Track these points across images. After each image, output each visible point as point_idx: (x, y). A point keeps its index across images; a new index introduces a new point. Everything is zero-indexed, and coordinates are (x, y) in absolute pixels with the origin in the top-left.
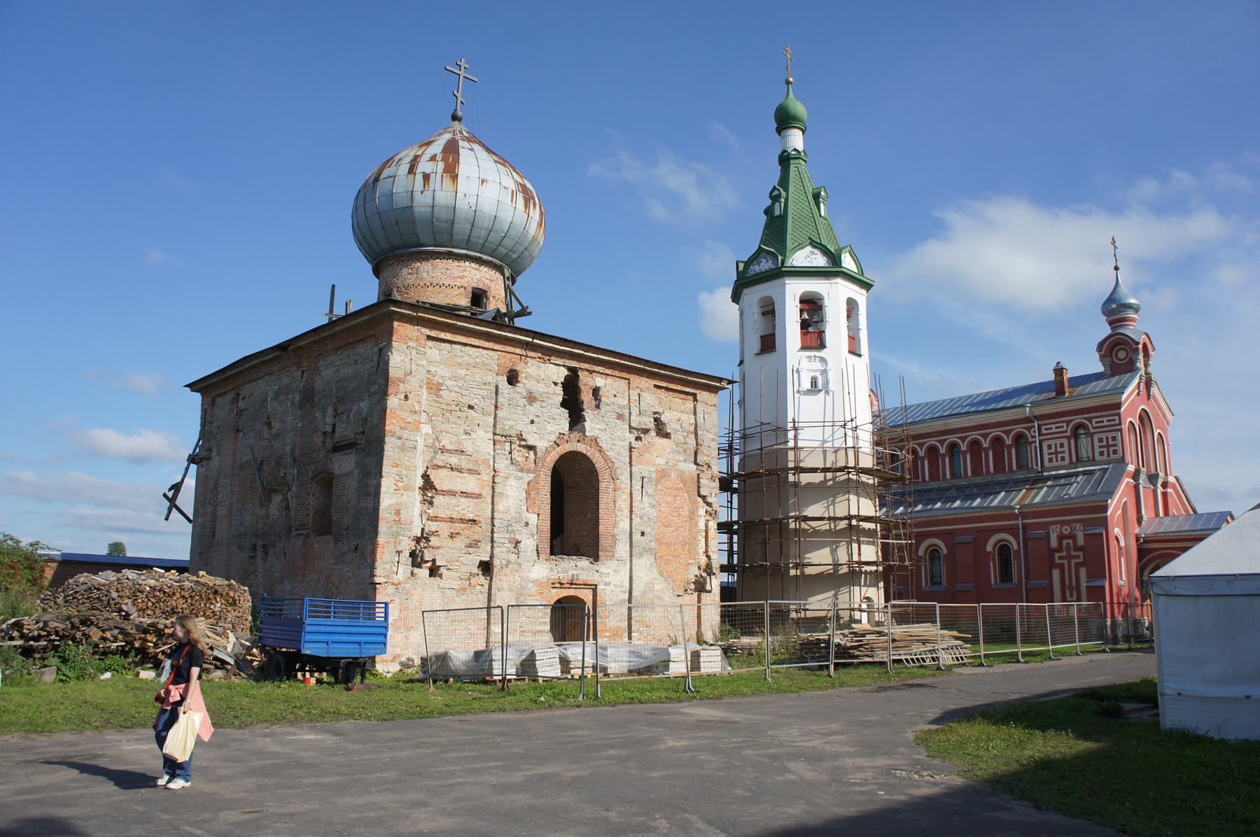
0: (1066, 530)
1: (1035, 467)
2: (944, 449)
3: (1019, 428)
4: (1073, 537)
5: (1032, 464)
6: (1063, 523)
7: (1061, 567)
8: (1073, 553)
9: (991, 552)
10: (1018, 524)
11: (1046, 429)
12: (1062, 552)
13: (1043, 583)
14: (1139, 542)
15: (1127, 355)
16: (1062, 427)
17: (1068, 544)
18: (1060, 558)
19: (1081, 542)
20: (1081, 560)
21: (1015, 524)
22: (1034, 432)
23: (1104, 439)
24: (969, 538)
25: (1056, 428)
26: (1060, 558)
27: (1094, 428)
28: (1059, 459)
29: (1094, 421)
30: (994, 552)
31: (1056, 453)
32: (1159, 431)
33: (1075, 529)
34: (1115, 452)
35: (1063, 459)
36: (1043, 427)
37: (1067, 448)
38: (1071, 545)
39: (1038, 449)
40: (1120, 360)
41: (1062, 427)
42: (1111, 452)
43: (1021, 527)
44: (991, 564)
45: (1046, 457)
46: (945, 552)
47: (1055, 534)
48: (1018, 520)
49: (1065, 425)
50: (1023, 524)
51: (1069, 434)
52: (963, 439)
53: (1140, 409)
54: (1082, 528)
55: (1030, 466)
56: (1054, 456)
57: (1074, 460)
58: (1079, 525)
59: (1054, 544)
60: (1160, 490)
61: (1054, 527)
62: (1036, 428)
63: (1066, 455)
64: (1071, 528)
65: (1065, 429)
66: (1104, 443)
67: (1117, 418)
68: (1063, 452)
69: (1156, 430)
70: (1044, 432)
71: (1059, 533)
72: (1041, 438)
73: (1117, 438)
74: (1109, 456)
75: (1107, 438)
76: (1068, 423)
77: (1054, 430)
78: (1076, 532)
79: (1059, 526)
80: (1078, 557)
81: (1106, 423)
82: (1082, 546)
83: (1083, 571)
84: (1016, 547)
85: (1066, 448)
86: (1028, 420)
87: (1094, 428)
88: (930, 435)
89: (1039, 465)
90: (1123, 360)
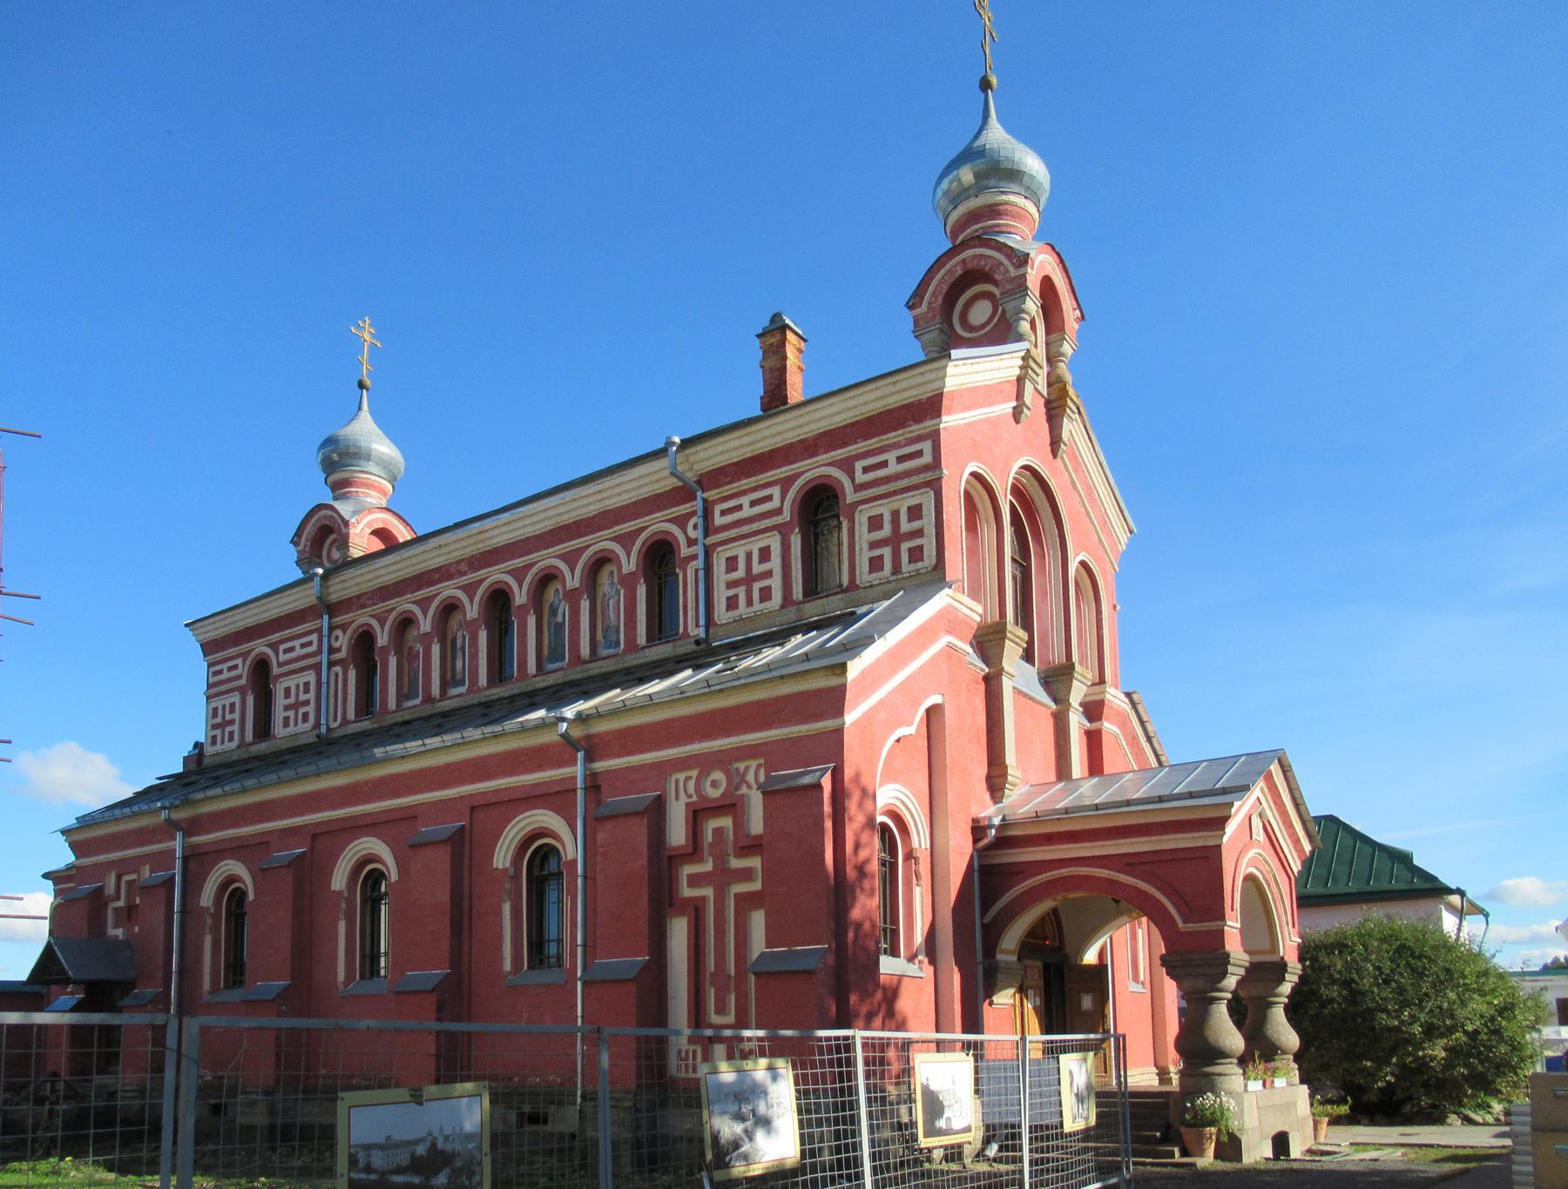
0: (716, 786)
2: (476, 607)
3: (657, 523)
4: (731, 806)
6: (705, 763)
7: (696, 911)
8: (736, 863)
10: (575, 778)
12: (701, 860)
16: (769, 498)
18: (694, 881)
23: (887, 518)
25: (753, 503)
26: (694, 881)
27: (858, 488)
28: (756, 595)
29: (859, 466)
31: (749, 579)
33: (743, 780)
34: (916, 554)
35: (766, 594)
36: (717, 509)
39: (701, 574)
41: (769, 498)
42: (905, 557)
45: (721, 595)
46: (394, 876)
47: (683, 799)
49: (776, 491)
51: (786, 516)
56: (741, 591)
57: (798, 591)
58: (753, 764)
60: (1077, 722)
61: (681, 776)
62: (700, 513)
63: (776, 583)
64: (729, 778)
65: (775, 503)
67: (927, 446)
68: (769, 574)
71: (695, 799)
72: (711, 540)
73: (925, 512)
75: (895, 515)
77: (747, 512)
78: (744, 790)
79: (694, 773)
80: (746, 874)
82: (760, 837)
85: (775, 563)
86: (682, 494)
87: (858, 488)
89: (702, 621)
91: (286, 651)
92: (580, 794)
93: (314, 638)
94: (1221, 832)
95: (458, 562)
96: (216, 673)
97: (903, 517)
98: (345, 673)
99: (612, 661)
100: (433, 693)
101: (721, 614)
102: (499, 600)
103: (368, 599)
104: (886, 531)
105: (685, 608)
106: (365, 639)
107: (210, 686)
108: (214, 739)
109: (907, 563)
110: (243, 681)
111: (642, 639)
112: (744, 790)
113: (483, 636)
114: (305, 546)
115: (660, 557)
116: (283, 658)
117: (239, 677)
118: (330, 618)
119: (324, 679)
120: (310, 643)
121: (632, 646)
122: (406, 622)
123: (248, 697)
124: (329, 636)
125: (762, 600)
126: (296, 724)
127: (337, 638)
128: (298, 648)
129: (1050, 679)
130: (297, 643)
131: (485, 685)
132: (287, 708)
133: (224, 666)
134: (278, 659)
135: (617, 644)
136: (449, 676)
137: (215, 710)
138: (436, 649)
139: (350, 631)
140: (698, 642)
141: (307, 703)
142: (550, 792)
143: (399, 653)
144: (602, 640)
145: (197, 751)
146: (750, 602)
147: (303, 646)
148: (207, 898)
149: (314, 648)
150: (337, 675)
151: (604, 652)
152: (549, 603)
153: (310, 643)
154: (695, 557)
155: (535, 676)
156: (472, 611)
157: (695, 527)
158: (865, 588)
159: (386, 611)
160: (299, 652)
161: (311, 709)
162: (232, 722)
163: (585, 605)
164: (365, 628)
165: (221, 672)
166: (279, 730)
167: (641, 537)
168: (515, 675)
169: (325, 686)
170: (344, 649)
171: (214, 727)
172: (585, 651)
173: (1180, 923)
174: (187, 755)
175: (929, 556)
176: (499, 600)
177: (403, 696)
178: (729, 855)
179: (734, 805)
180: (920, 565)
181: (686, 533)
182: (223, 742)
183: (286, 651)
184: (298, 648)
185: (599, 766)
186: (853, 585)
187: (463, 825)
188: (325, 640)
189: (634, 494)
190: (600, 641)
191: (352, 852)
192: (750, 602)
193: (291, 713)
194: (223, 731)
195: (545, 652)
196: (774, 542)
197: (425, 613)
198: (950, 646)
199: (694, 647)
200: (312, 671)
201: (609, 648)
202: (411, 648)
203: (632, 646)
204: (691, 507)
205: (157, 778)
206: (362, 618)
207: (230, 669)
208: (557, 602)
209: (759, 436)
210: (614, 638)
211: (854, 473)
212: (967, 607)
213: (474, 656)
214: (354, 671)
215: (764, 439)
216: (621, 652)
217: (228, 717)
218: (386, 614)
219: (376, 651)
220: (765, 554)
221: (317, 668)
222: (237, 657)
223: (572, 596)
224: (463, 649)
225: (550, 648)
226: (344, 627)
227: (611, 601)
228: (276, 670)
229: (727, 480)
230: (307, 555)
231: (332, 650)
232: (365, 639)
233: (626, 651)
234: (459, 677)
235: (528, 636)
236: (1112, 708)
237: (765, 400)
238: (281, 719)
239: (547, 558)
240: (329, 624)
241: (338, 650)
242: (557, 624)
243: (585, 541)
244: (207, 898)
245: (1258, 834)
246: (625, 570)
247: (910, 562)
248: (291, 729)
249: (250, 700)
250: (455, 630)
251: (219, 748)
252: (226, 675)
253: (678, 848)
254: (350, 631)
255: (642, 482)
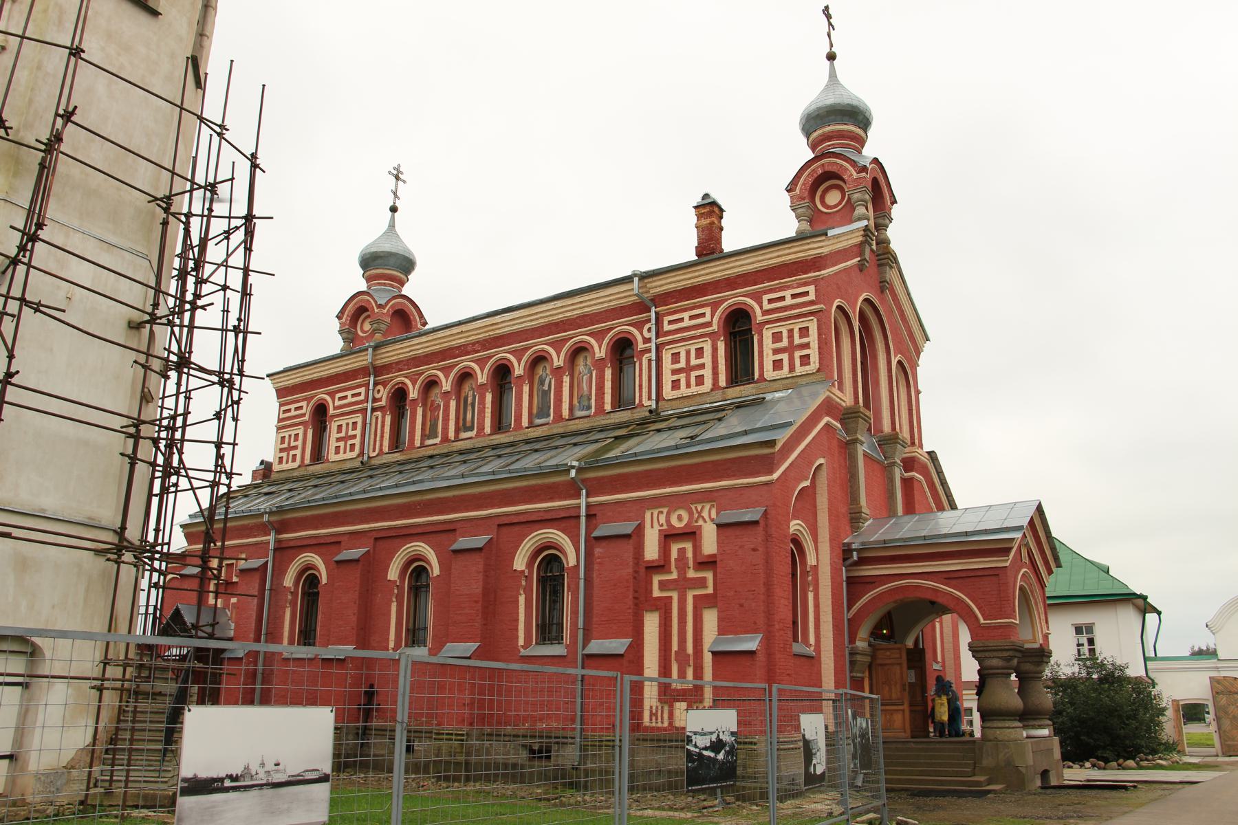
0: (679, 520)
1: (646, 402)
2: (485, 376)
3: (622, 326)
4: (691, 534)
5: (641, 396)
8: (691, 574)
9: (523, 572)
10: (579, 507)
11: (670, 322)
12: (670, 572)
13: (618, 645)
14: (849, 562)
15: (843, 198)
16: (703, 315)
17: (682, 552)
18: (663, 586)
19: (710, 543)
20: (710, 590)
21: (568, 508)
22: (649, 330)
23: (785, 334)
24: (479, 541)
25: (692, 318)
27: (765, 313)
29: (765, 298)
30: (531, 572)
31: (688, 369)
32: (899, 357)
33: (700, 516)
35: (700, 380)
36: (666, 319)
37: (710, 357)
38: (690, 554)
39: (654, 364)
40: (828, 207)
41: (703, 315)
43: (583, 512)
44: (522, 599)
45: (668, 379)
46: (436, 571)
48: (578, 496)
49: (708, 311)
50: (588, 506)
51: (715, 327)
52: (519, 354)
53: (861, 299)
54: (714, 515)
55: (637, 401)
57: (722, 382)
59: (651, 551)
60: (898, 473)
62: (653, 321)
63: (707, 373)
64: (691, 513)
65: (707, 318)
66: (785, 343)
68: (702, 366)
69: (895, 356)
70: (667, 327)
71: (665, 527)
72: (661, 340)
73: (810, 332)
74: (792, 368)
76: (715, 306)
77: (687, 323)
78: (701, 522)
80: (702, 583)
81: (789, 301)
82: (714, 556)
83: (711, 619)
84: (571, 561)
85: (707, 359)
86: (641, 307)
88: (463, 350)
89: (654, 397)
90: (835, 206)
91: (340, 399)
92: (583, 520)
93: (362, 390)
94: (1007, 558)
95: (474, 344)
96: (285, 412)
97: (796, 335)
98: (383, 418)
99: (586, 420)
100: (450, 435)
101: (668, 392)
102: (502, 372)
103: (404, 365)
104: (785, 343)
105: (641, 386)
106: (400, 395)
107: (280, 420)
108: (281, 458)
109: (799, 365)
110: (306, 418)
111: (608, 407)
112: (701, 522)
113: (489, 397)
114: (346, 320)
115: (623, 349)
116: (338, 403)
117: (303, 415)
118: (375, 377)
119: (368, 421)
120: (359, 394)
121: (600, 410)
122: (432, 384)
123: (309, 430)
124: (373, 390)
125: (697, 385)
126: (345, 452)
127: (379, 391)
128: (349, 396)
129: (882, 443)
130: (349, 393)
131: (489, 432)
132: (338, 440)
133: (292, 407)
134: (334, 403)
135: (589, 408)
136: (461, 424)
137: (283, 438)
138: (453, 404)
139: (389, 387)
140: (651, 412)
141: (354, 437)
142: (558, 517)
143: (424, 405)
144: (578, 404)
145: (263, 467)
146: (688, 386)
147: (353, 396)
148: (288, 581)
149: (362, 397)
150: (377, 418)
151: (579, 413)
152: (538, 376)
153: (359, 394)
154: (649, 351)
155: (527, 428)
156: (482, 377)
157: (649, 330)
158: (770, 381)
159: (417, 375)
160: (350, 400)
161: (357, 441)
162: (295, 448)
163: (566, 379)
164: (400, 385)
165: (289, 410)
166: (332, 457)
167: (609, 335)
168: (512, 426)
169: (368, 426)
170: (384, 399)
171: (282, 450)
172: (565, 413)
173: (982, 621)
174: (255, 469)
175: (814, 363)
176: (502, 372)
177: (425, 436)
178: (689, 568)
179: (694, 533)
180: (807, 368)
181: (642, 334)
182: (287, 462)
183: (340, 399)
184: (349, 396)
185: (592, 500)
186: (762, 379)
187: (492, 538)
188: (371, 392)
189: (606, 305)
190: (575, 405)
191: (406, 552)
192: (688, 386)
193: (341, 444)
194: (288, 454)
195: (535, 411)
196: (707, 347)
197: (447, 377)
198: (827, 425)
199: (647, 414)
200: (359, 415)
201: (582, 410)
202: (433, 401)
203: (600, 410)
204: (646, 317)
205: (238, 487)
206: (400, 378)
207: (296, 409)
208: (544, 375)
209: (697, 274)
210: (586, 404)
211: (762, 303)
212: (838, 397)
213: (482, 411)
214: (390, 417)
215: (700, 276)
216: (592, 414)
217: (293, 444)
218: (417, 377)
219: (408, 402)
220: (700, 352)
221: (364, 411)
222: (303, 400)
223: (558, 372)
224: (473, 405)
225: (538, 407)
226: (384, 384)
227: (585, 377)
228: (331, 412)
229: (673, 300)
230: (347, 327)
231: (375, 400)
232: (400, 395)
233: (596, 414)
234: (468, 424)
235: (522, 400)
236: (919, 463)
237: (699, 249)
238: (334, 448)
239: (540, 345)
240: (374, 381)
241: (380, 400)
242: (543, 390)
243: (569, 335)
244: (288, 581)
245: (1025, 558)
246: (597, 355)
247: (801, 365)
248: (341, 456)
249: (310, 433)
250: (467, 391)
251: (284, 466)
252: (293, 413)
253: (653, 561)
254: (389, 387)
255: (612, 298)
